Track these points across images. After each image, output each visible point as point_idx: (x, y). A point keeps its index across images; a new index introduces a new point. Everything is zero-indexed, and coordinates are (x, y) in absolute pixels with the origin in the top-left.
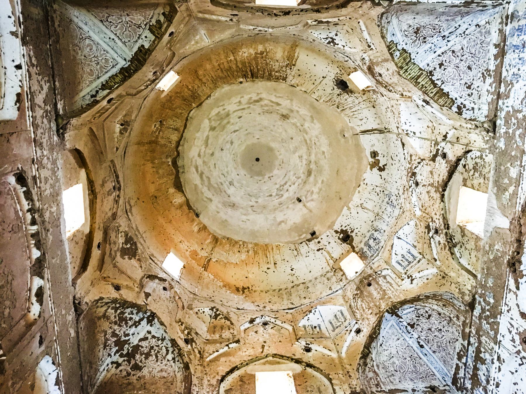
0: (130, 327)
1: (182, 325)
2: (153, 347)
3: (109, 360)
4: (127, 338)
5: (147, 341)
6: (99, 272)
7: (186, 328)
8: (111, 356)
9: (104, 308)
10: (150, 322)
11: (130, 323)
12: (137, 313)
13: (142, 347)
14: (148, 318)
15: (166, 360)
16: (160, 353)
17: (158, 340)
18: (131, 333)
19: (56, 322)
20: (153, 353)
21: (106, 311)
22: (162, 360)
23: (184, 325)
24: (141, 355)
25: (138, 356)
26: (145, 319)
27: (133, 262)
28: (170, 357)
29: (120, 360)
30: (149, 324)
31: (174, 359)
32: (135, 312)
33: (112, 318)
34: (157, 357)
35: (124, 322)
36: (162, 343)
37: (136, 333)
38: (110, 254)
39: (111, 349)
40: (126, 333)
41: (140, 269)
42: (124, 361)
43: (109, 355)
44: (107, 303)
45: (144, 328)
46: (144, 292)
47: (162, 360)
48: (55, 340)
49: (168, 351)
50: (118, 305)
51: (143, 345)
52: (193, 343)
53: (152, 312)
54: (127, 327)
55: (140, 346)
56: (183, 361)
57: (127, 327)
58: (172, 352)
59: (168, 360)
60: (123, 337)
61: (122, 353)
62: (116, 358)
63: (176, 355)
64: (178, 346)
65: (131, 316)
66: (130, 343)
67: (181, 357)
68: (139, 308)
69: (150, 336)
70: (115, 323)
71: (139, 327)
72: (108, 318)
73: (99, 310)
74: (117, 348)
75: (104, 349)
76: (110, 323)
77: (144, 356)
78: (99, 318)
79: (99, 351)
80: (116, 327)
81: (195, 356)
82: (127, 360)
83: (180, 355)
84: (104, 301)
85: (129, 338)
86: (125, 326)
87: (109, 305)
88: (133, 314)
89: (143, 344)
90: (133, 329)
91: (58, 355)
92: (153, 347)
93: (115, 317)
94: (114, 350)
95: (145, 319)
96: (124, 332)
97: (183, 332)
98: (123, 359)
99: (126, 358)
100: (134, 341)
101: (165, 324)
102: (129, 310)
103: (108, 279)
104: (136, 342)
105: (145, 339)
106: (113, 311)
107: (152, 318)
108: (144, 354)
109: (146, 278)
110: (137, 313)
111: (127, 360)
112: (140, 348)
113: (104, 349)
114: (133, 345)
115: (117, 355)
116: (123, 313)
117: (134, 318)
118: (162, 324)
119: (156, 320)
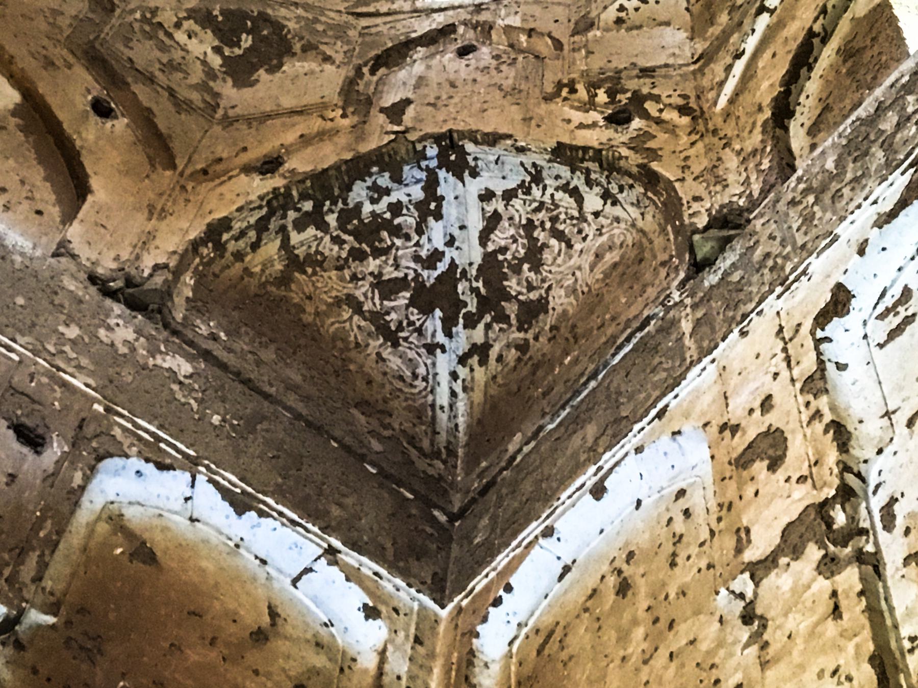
0: (420, 231)
1: (573, 91)
2: (530, 221)
3: (444, 363)
4: (442, 267)
5: (505, 223)
6: (168, 173)
7: (593, 86)
8: (443, 349)
9: (271, 247)
10: (461, 168)
11: (408, 220)
12: (398, 179)
13: (503, 250)
14: (444, 162)
15: (590, 218)
16: (562, 217)
17: (528, 192)
18: (439, 242)
19: (59, 369)
20: (540, 236)
21: (285, 244)
22: (580, 231)
23: (580, 87)
24: (517, 270)
25: (513, 285)
26: (442, 174)
27: (292, 67)
28: (593, 201)
29: (478, 335)
30: (467, 173)
31: (606, 196)
32: (384, 181)
33: (329, 249)
34: (559, 235)
35: (385, 234)
36: (545, 188)
37: (456, 233)
38: (181, 106)
39: (420, 331)
40: (424, 253)
41: (328, 67)
42: (488, 327)
43: (431, 349)
44: (262, 226)
45: (462, 201)
46: (382, 110)
47: (580, 231)
48: (108, 410)
49: (575, 193)
50: (308, 206)
51: (503, 243)
52: (650, 106)
53: (437, 139)
54: (408, 238)
55: (495, 252)
56: (630, 175)
57: (408, 238)
58: (589, 183)
59: (596, 214)
60: (425, 274)
61: (467, 316)
62: (463, 339)
63: (603, 180)
64: (585, 149)
65: (386, 200)
66: (464, 272)
67: (619, 170)
68: (390, 161)
69: (498, 205)
70: (358, 255)
71: (450, 210)
72: (316, 261)
73: (255, 262)
74: (438, 313)
75: (396, 344)
76: (340, 268)
77: (526, 266)
78: (284, 280)
79: (380, 358)
80: (373, 264)
81: (673, 130)
82: (495, 319)
83: (611, 167)
84: (237, 226)
85: (447, 260)
86: (398, 242)
87: (274, 224)
88: (388, 192)
89: (499, 238)
90: (437, 233)
91: (159, 439)
92: (530, 221)
93: (336, 240)
94: (434, 323)
95: (442, 174)
96: (417, 258)
97: (590, 105)
98: (481, 327)
99: (488, 318)
100: (470, 254)
101: (503, 130)
102: (359, 192)
103: (219, 168)
104: (476, 255)
105: (493, 222)
106: (311, 231)
107: (453, 154)
108: (522, 261)
109: (373, 72)
110: (398, 179)
111: (495, 319)
112: (500, 257)
113: (396, 344)
114: (475, 266)
115: (459, 328)
116: (349, 215)
117: (405, 199)
118: (492, 139)
119: (470, 147)
